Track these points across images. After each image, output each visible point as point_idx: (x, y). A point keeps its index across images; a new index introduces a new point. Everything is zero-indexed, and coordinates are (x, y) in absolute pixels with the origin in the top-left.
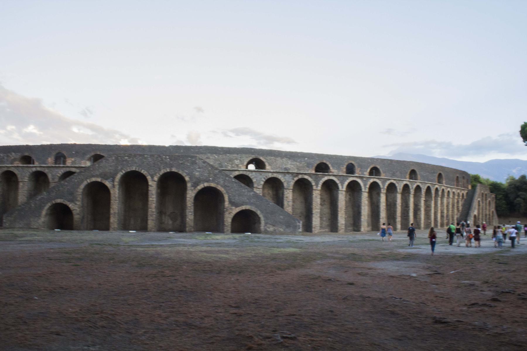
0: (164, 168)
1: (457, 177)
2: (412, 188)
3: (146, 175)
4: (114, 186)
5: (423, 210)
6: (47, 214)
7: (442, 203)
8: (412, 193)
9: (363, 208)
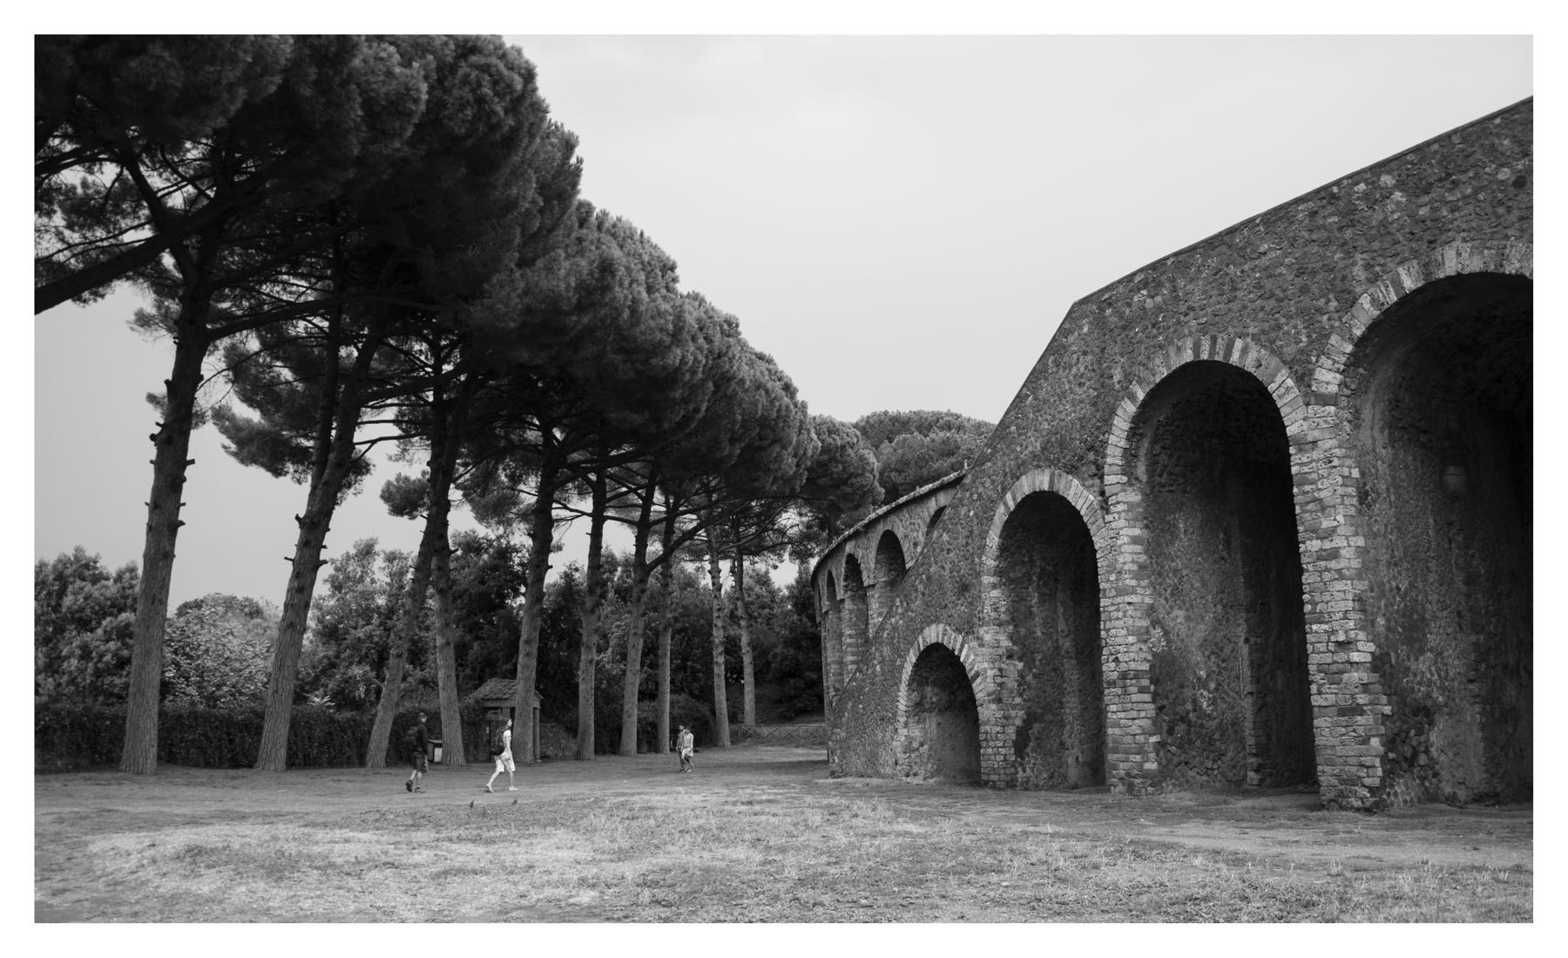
0: (1373, 280)
3: (1260, 375)
4: (1106, 501)
6: (918, 709)
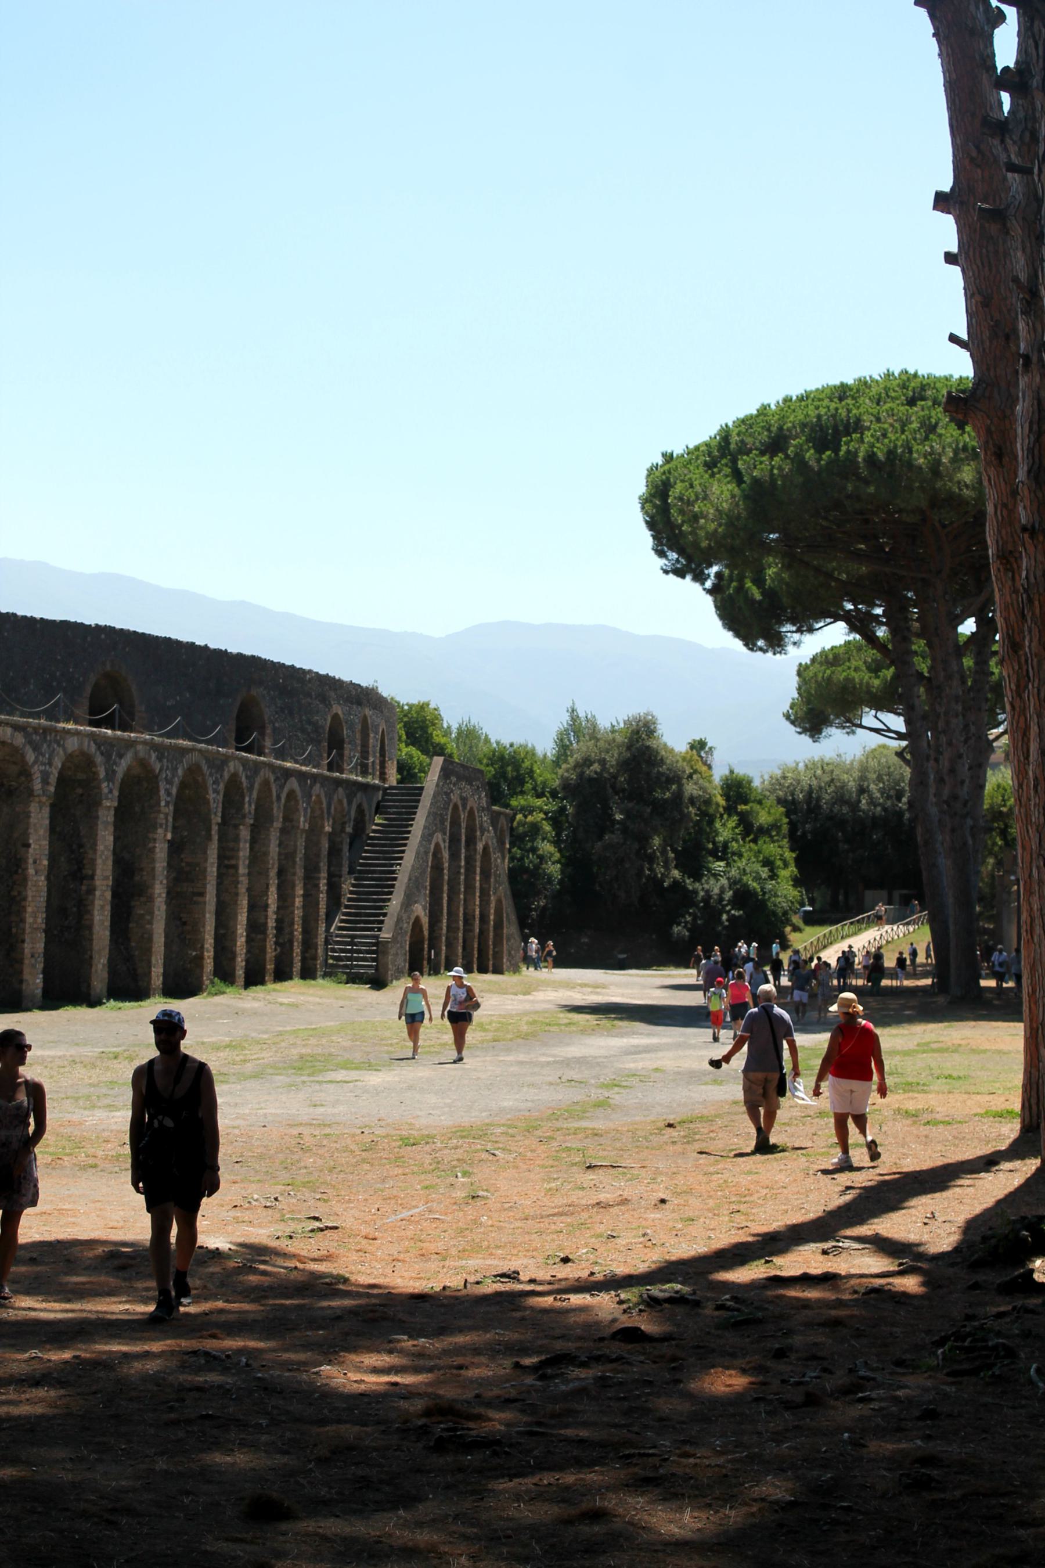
2: (110, 776)
5: (159, 890)
7: (257, 859)
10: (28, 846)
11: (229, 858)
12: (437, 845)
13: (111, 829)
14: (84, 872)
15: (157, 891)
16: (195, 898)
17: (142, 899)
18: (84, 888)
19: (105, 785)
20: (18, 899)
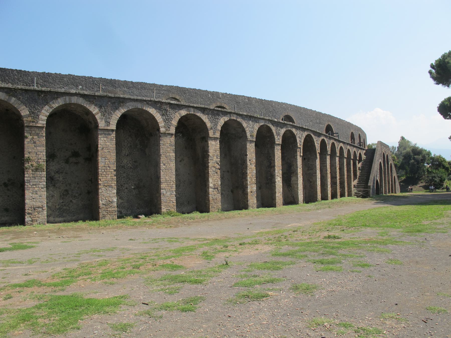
1: (352, 133)
2: (278, 134)
8: (278, 143)
9: (162, 167)
10: (247, 155)
11: (324, 164)
12: (380, 162)
13: (280, 151)
14: (272, 165)
15: (299, 171)
16: (314, 175)
17: (294, 174)
18: (272, 170)
19: (276, 137)
20: (245, 173)
